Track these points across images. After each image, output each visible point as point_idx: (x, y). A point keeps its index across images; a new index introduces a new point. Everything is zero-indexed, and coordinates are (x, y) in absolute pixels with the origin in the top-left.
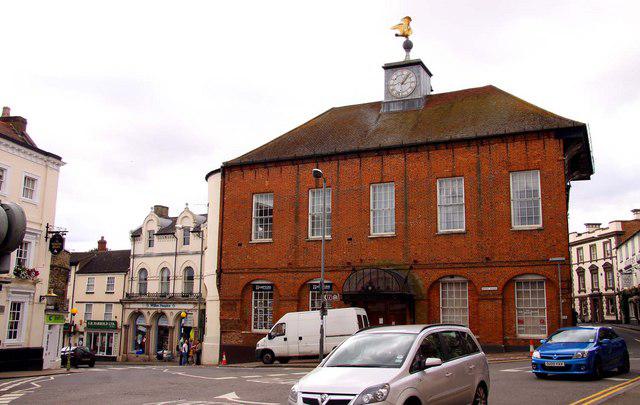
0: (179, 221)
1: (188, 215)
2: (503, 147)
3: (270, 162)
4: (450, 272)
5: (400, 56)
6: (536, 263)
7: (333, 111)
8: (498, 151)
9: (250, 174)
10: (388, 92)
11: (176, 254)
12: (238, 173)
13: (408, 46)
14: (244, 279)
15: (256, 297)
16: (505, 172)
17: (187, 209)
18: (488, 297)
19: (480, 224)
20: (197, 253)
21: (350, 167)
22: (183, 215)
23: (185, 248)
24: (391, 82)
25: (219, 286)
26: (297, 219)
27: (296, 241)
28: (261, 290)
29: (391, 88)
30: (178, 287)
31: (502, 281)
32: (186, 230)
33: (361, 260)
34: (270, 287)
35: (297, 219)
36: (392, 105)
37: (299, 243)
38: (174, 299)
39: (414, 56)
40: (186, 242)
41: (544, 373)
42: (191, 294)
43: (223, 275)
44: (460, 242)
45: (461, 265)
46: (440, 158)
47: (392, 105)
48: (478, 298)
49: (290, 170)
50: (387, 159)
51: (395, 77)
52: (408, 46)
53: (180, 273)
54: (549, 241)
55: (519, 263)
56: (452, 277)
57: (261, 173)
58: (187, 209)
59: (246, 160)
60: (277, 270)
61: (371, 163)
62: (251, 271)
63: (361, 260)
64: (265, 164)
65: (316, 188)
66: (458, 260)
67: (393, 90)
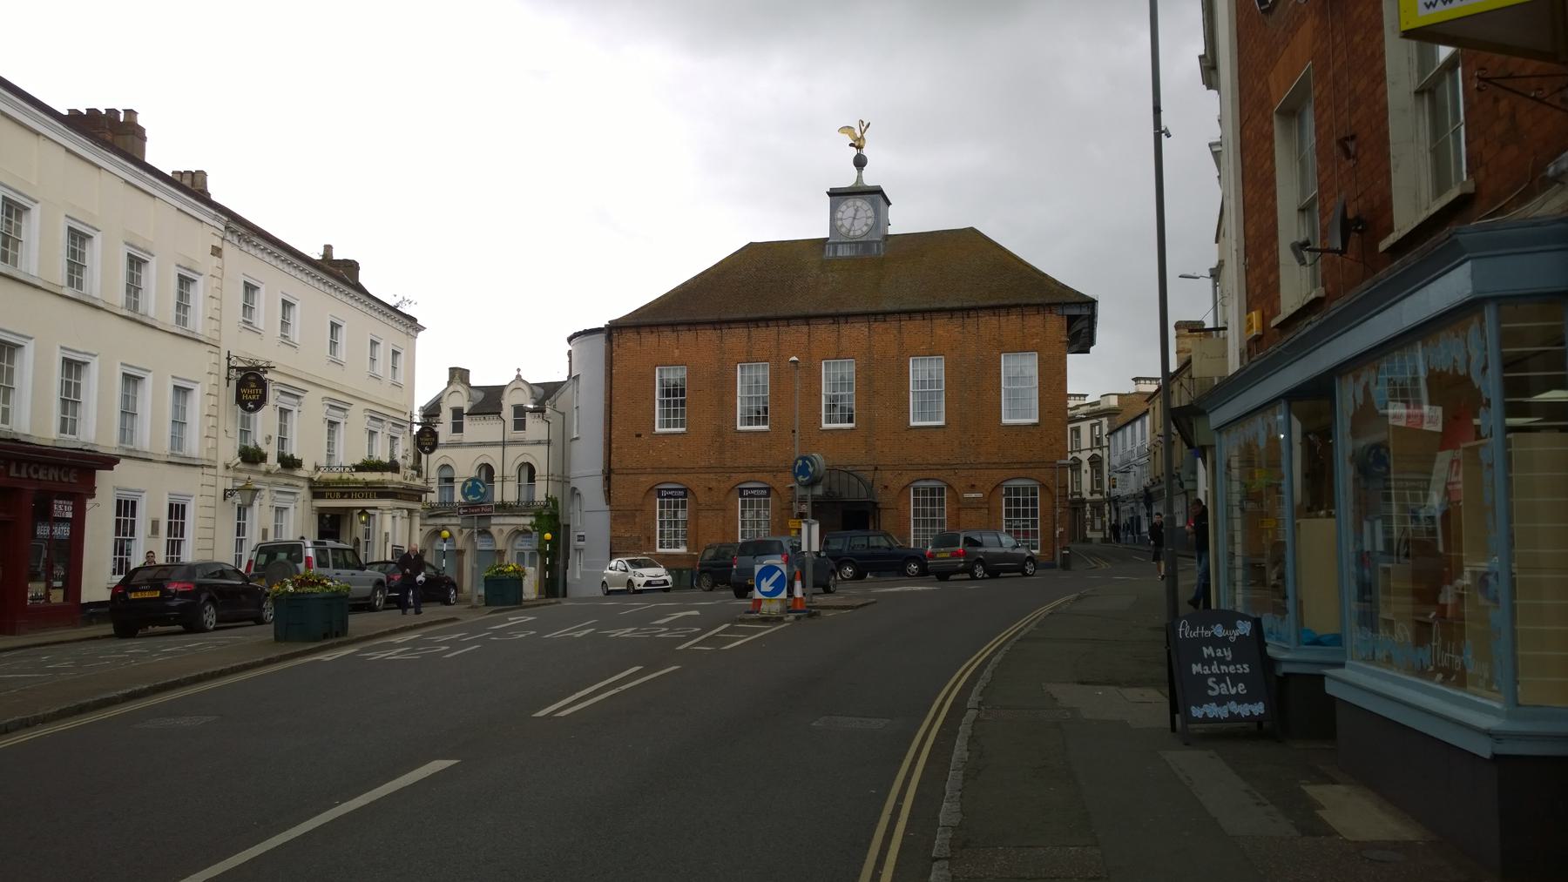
1: (521, 385)
2: (994, 321)
4: (927, 474)
5: (847, 178)
8: (989, 323)
9: (650, 339)
11: (504, 444)
12: (631, 335)
13: (860, 162)
14: (646, 481)
15: (662, 506)
17: (519, 377)
18: (974, 506)
20: (539, 443)
21: (796, 335)
23: (519, 435)
24: (839, 215)
31: (989, 487)
32: (519, 411)
37: (723, 433)
39: (870, 178)
40: (520, 425)
49: (708, 335)
52: (860, 162)
53: (512, 471)
57: (668, 337)
58: (519, 377)
61: (823, 332)
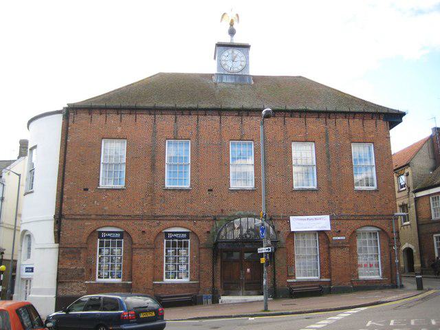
2: (346, 121)
3: (125, 108)
5: (227, 39)
6: (375, 217)
7: (161, 76)
8: (342, 123)
9: (98, 118)
10: (220, 66)
12: (84, 116)
13: (232, 32)
14: (90, 225)
15: (101, 245)
16: (348, 142)
18: (340, 245)
19: (330, 183)
21: (211, 122)
24: (223, 58)
25: (58, 237)
26: (153, 167)
27: (151, 190)
29: (224, 63)
31: (349, 232)
33: (222, 210)
34: (118, 235)
35: (153, 167)
36: (225, 77)
37: (155, 190)
39: (237, 40)
43: (63, 221)
44: (314, 197)
46: (294, 123)
47: (225, 77)
49: (145, 118)
50: (247, 120)
51: (226, 54)
52: (232, 32)
57: (113, 118)
59: (93, 104)
61: (231, 121)
63: (222, 210)
64: (118, 110)
65: (175, 139)
67: (225, 64)
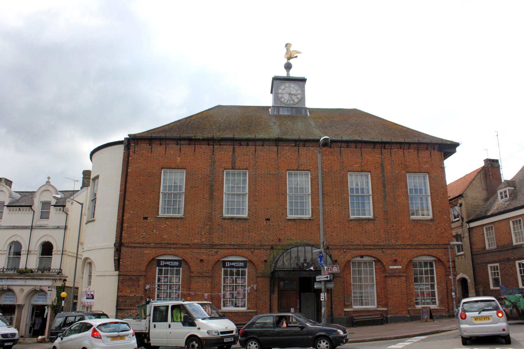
0: (37, 195)
1: (50, 188)
2: (401, 152)
4: (362, 252)
5: (283, 73)
6: (432, 247)
7: (219, 107)
9: (158, 149)
10: (276, 99)
11: (32, 228)
12: (145, 146)
13: (288, 67)
14: (150, 253)
16: (403, 172)
17: (48, 182)
18: (395, 274)
19: (386, 212)
20: (58, 228)
21: (267, 153)
22: (44, 188)
23: (44, 222)
24: (280, 91)
25: (118, 265)
26: (211, 197)
27: (210, 218)
28: (232, 267)
29: (280, 96)
30: (31, 261)
31: (405, 261)
32: (46, 205)
33: (280, 240)
34: (176, 263)
35: (211, 197)
36: (281, 109)
38: (26, 273)
39: (294, 73)
40: (45, 215)
41: (467, 341)
42: (49, 269)
43: (124, 249)
44: (370, 226)
45: (372, 247)
46: (350, 155)
47: (281, 109)
48: (385, 275)
49: (204, 149)
50: (303, 150)
51: (283, 87)
52: (288, 67)
53: (36, 248)
54: (439, 230)
55: (417, 247)
56: (362, 257)
57: (173, 149)
58: (48, 182)
59: (154, 135)
60: (188, 246)
61: (287, 151)
62: (159, 245)
63: (280, 240)
64: (178, 140)
65: (233, 168)
66: (369, 242)
67: (281, 97)
